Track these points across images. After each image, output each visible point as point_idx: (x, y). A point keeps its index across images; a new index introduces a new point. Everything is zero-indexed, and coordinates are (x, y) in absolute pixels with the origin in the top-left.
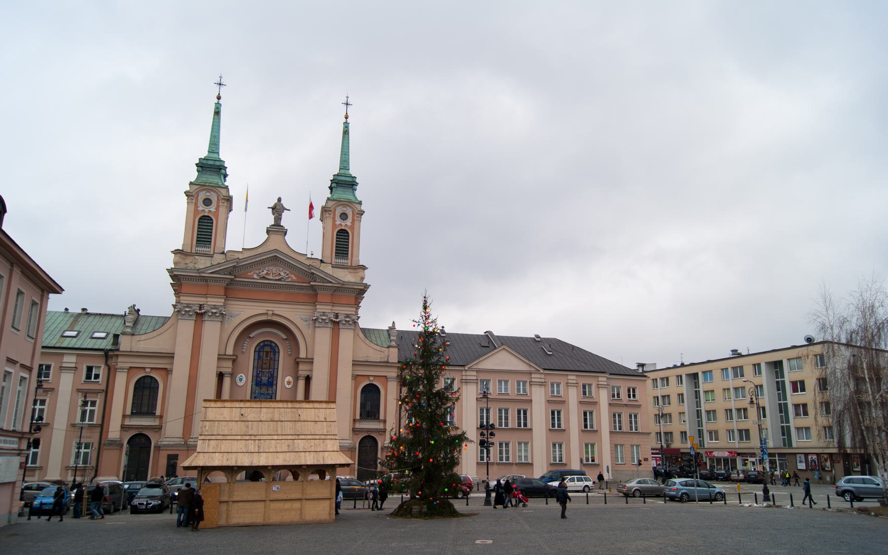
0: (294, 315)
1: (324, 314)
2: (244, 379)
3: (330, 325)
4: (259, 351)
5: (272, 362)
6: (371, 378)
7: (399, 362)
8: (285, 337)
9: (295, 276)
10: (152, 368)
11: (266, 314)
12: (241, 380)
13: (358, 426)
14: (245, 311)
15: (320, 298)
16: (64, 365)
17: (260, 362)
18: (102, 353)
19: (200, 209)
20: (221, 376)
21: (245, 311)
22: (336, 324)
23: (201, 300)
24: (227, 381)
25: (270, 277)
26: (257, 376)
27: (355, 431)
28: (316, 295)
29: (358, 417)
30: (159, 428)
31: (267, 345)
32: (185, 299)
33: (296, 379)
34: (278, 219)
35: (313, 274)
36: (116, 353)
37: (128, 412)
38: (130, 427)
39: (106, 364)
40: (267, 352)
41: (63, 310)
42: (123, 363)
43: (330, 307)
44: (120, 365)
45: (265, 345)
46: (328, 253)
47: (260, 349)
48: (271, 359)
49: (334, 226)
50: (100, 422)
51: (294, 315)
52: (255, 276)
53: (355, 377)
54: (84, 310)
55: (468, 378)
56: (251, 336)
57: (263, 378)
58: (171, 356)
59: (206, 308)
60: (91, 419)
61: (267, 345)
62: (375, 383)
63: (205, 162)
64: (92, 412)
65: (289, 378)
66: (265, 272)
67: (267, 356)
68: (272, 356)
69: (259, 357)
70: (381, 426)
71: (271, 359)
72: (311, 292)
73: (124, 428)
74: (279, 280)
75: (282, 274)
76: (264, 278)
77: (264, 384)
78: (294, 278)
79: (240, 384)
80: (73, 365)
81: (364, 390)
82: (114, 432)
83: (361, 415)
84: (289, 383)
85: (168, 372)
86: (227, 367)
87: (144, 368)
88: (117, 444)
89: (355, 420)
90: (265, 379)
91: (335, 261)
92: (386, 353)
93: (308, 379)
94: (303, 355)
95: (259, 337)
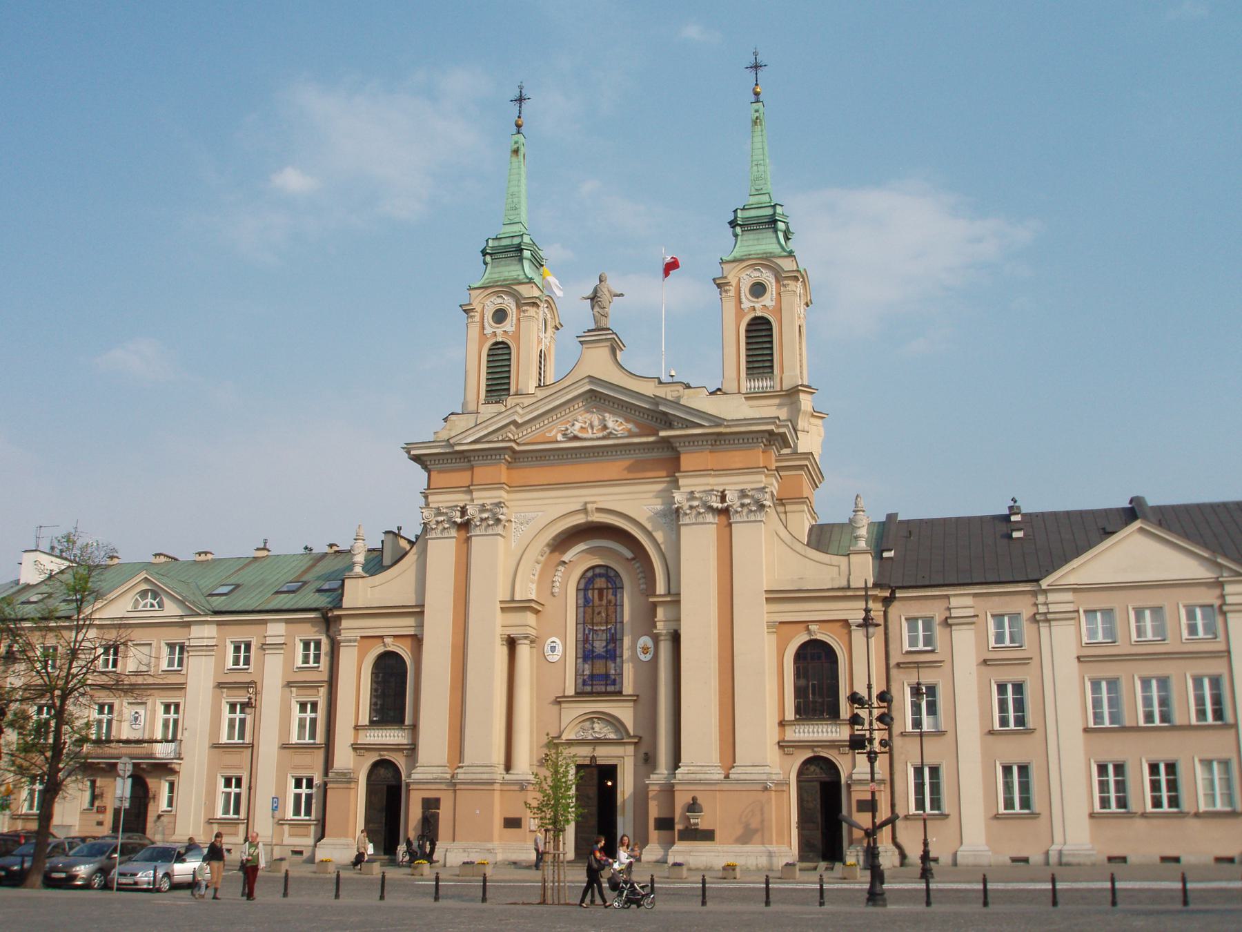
2: (560, 648)
4: (586, 589)
5: (611, 609)
6: (813, 627)
7: (876, 586)
8: (629, 555)
9: (636, 424)
11: (584, 510)
12: (553, 649)
15: (687, 461)
17: (590, 610)
19: (488, 330)
20: (512, 643)
21: (537, 512)
23: (460, 499)
25: (590, 435)
26: (586, 640)
27: (783, 745)
28: (678, 459)
29: (790, 715)
30: (412, 750)
31: (600, 575)
32: (437, 500)
33: (656, 639)
35: (665, 414)
36: (336, 613)
37: (364, 719)
38: (368, 748)
39: (328, 636)
40: (601, 591)
41: (303, 551)
42: (349, 629)
44: (344, 635)
45: (595, 576)
46: (731, 373)
47: (588, 582)
48: (609, 602)
49: (740, 312)
51: (635, 503)
52: (560, 437)
53: (782, 627)
54: (331, 546)
55: (1053, 608)
57: (597, 644)
58: (418, 612)
59: (471, 510)
60: (313, 736)
61: (600, 575)
62: (819, 637)
63: (496, 243)
64: (313, 721)
65: (646, 641)
66: (578, 425)
67: (601, 599)
68: (611, 597)
69: (587, 601)
71: (609, 602)
72: (667, 454)
74: (604, 438)
75: (610, 424)
76: (576, 438)
77: (599, 657)
78: (635, 430)
79: (554, 658)
81: (800, 655)
82: (344, 758)
83: (798, 710)
84: (645, 650)
85: (417, 641)
87: (382, 637)
89: (782, 724)
90: (599, 646)
91: (745, 385)
92: (844, 567)
93: (676, 638)
94: (661, 588)
95: (580, 558)
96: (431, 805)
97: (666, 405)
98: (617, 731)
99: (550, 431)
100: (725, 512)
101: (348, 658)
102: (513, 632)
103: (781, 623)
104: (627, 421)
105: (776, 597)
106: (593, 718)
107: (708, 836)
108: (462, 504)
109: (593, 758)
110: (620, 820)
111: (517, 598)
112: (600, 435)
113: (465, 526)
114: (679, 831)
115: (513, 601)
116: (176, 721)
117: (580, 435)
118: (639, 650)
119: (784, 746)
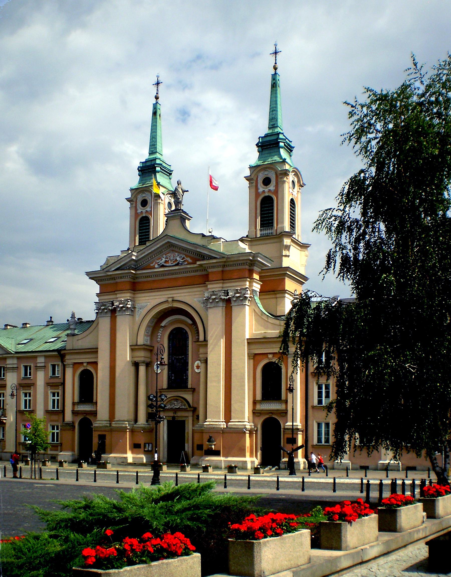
0: (190, 297)
1: (213, 293)
3: (221, 304)
8: (190, 322)
9: (191, 258)
10: (88, 363)
11: (167, 301)
13: (258, 407)
14: (150, 302)
16: (38, 365)
18: (56, 353)
20: (136, 365)
22: (228, 301)
24: (142, 369)
25: (170, 264)
34: (178, 202)
42: (70, 359)
43: (221, 285)
50: (62, 409)
51: (190, 297)
53: (254, 357)
56: (163, 324)
66: (164, 260)
70: (283, 407)
73: (74, 413)
74: (176, 265)
75: (178, 259)
76: (163, 266)
78: (190, 261)
80: (43, 365)
84: (198, 367)
86: (141, 356)
87: (82, 363)
88: (71, 426)
96: (102, 438)
97: (200, 249)
98: (185, 405)
99: (152, 263)
100: (228, 301)
101: (69, 372)
102: (137, 359)
103: (256, 354)
104: (187, 256)
105: (251, 342)
106: (176, 399)
107: (217, 453)
108: (112, 300)
109: (174, 417)
110: (186, 445)
111: (138, 344)
112: (174, 264)
113: (114, 311)
114: (205, 450)
115: (137, 345)
116: (3, 400)
117: (165, 264)
118: (195, 367)
119: (255, 413)
